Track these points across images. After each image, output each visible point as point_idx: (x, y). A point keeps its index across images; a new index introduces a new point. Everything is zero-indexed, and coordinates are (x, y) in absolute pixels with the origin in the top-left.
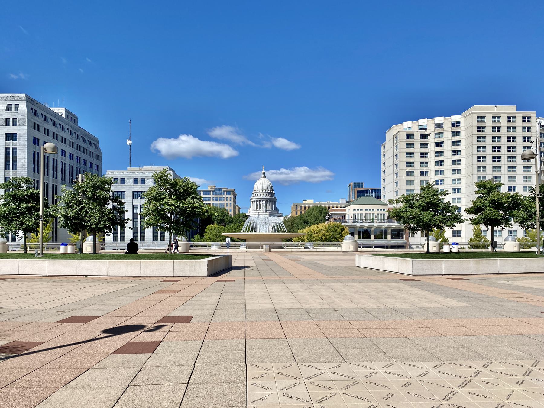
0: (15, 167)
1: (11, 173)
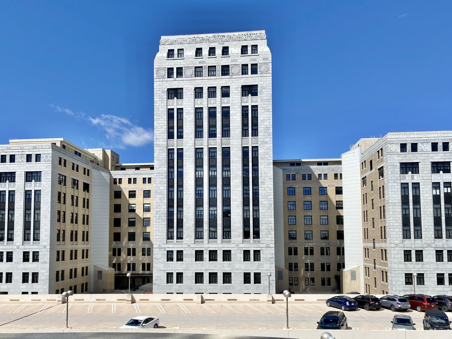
0: (255, 133)
1: (250, 140)
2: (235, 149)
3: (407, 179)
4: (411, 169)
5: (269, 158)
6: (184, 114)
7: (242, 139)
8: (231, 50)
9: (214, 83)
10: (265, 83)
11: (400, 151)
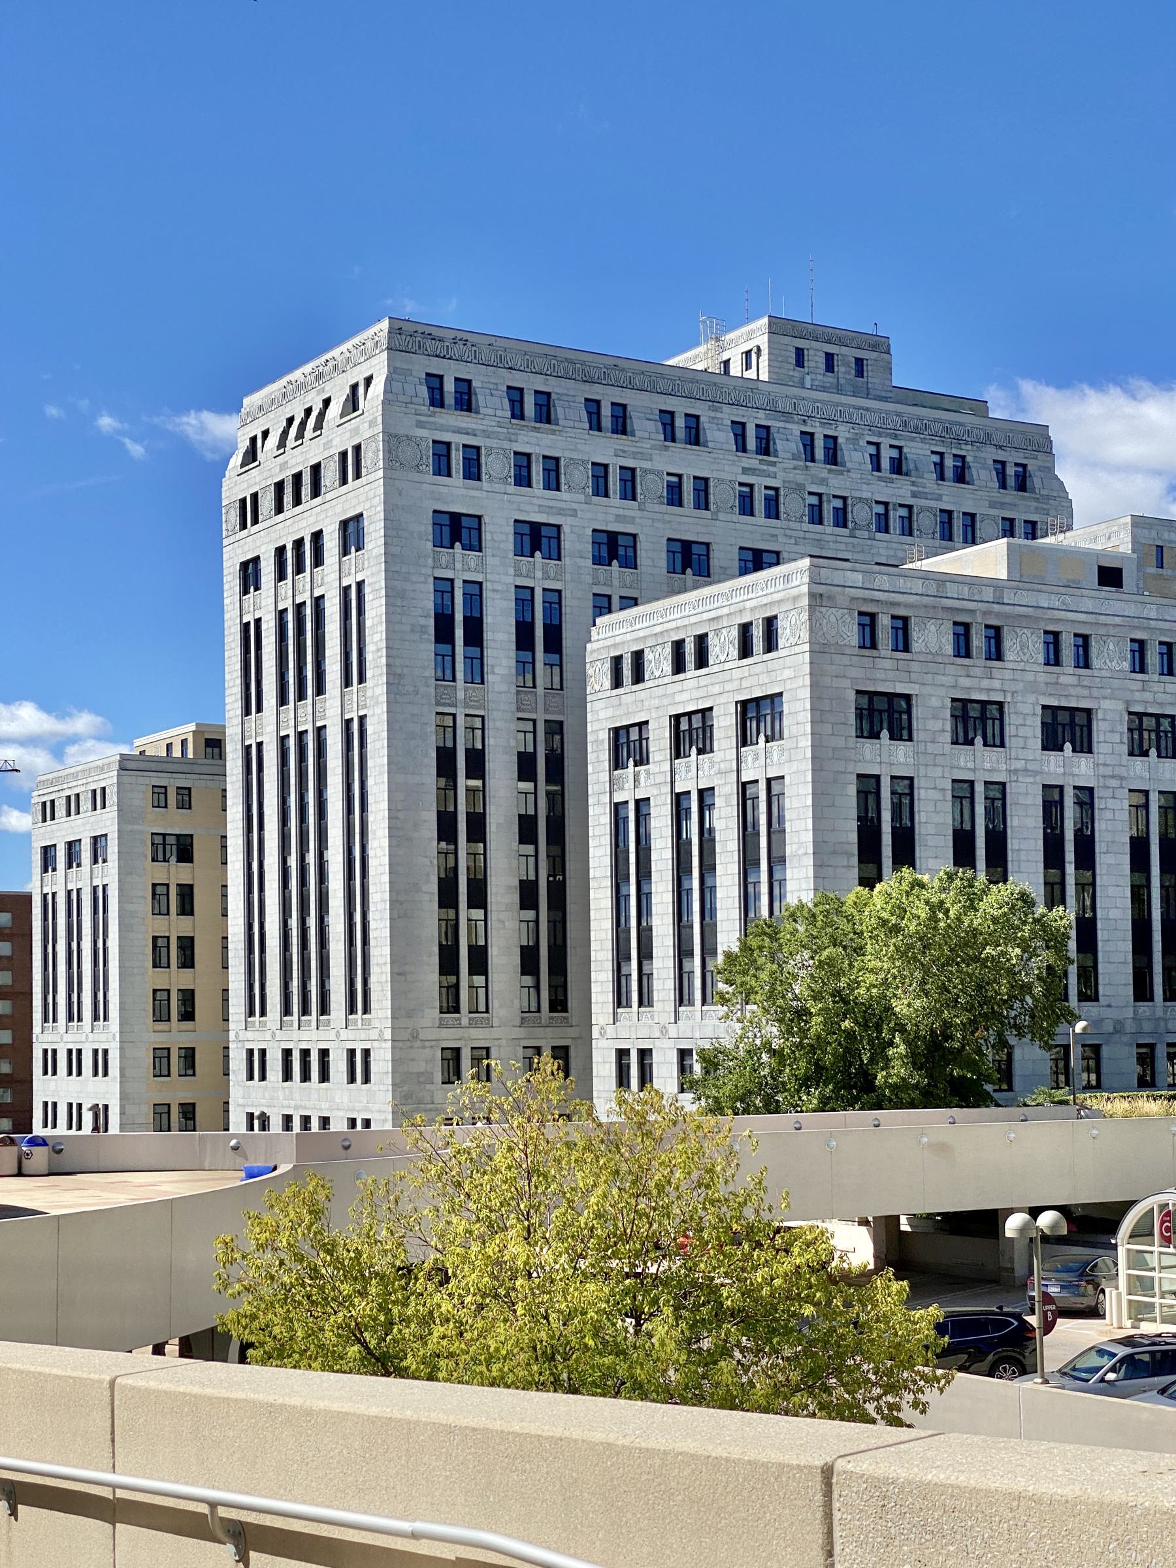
7: (342, 696)
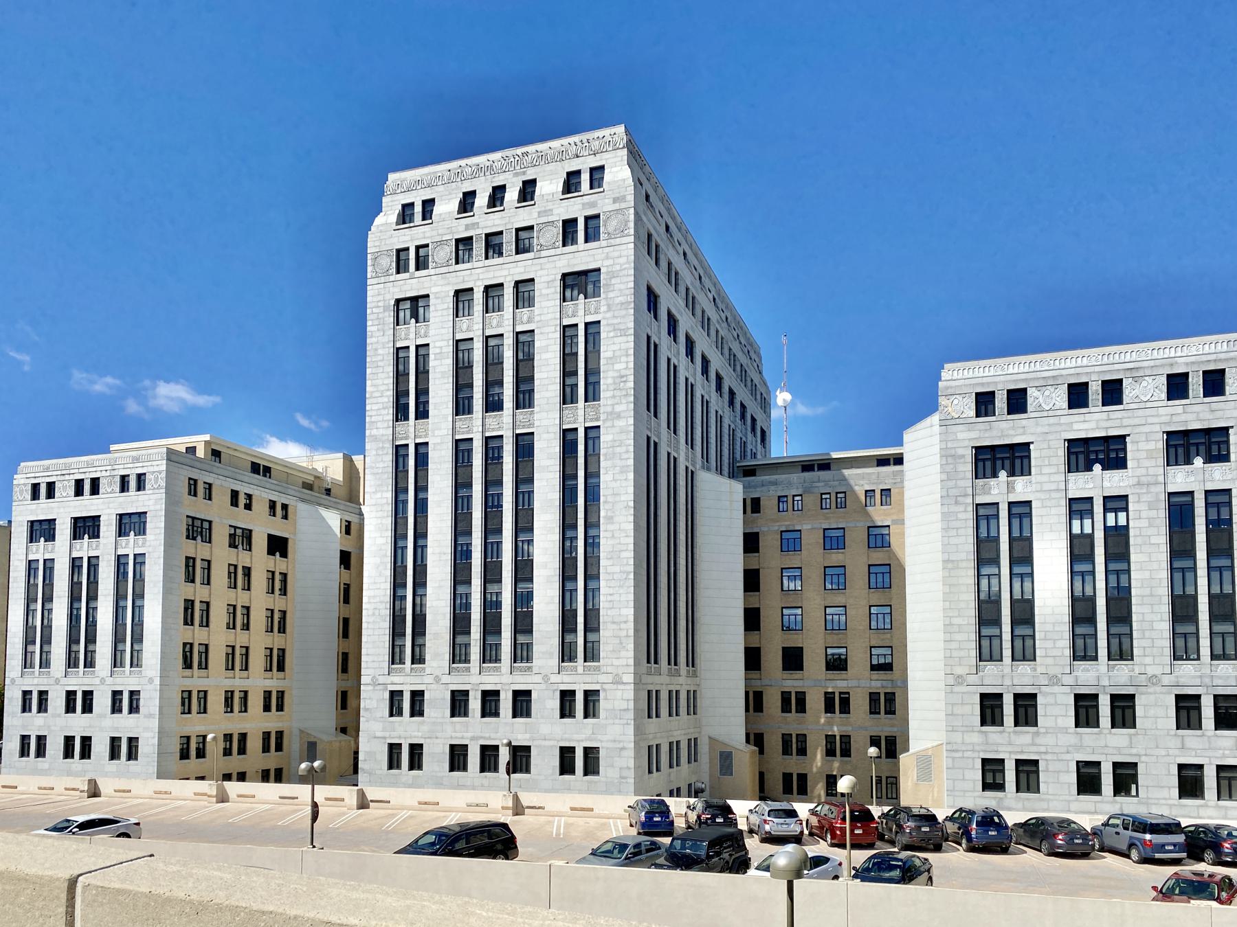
0: (592, 393)
1: (581, 412)
2: (545, 436)
3: (995, 491)
4: (1007, 463)
5: (625, 456)
6: (432, 357)
8: (542, 189)
9: (498, 274)
10: (617, 261)
11: (973, 413)
